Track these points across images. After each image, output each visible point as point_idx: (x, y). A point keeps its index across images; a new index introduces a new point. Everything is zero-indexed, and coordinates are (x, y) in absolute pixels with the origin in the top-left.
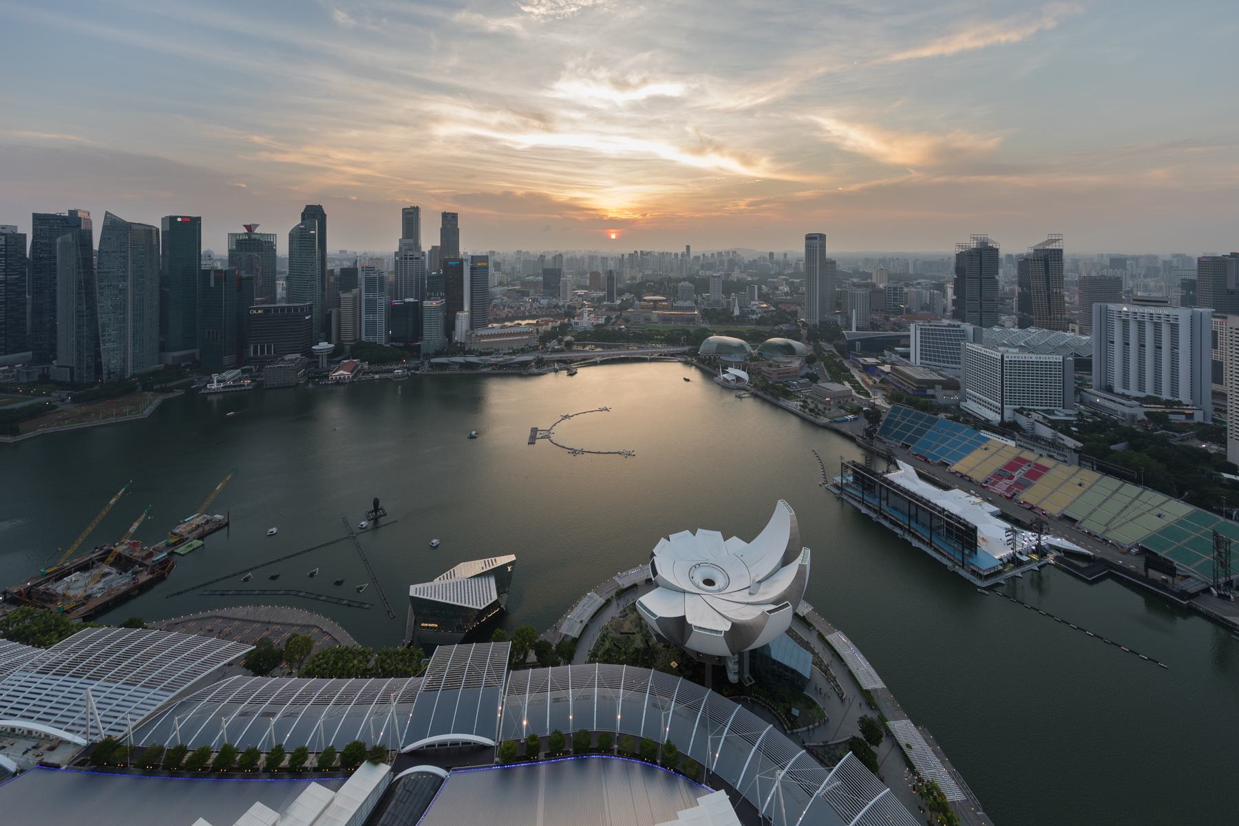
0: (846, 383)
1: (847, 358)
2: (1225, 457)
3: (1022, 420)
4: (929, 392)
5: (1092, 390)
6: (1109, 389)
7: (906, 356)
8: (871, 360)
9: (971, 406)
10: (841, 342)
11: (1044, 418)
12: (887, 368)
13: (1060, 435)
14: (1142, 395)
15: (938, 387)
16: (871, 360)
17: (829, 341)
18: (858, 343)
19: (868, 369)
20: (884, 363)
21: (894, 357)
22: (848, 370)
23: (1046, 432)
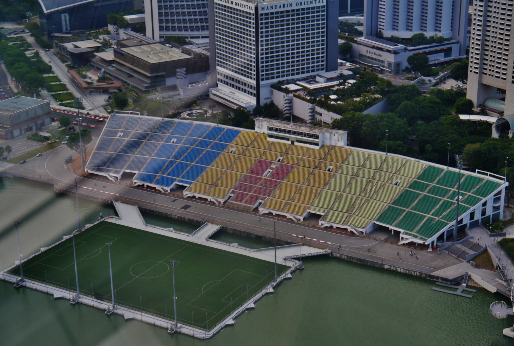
0: (44, 92)
1: (47, 47)
2: (465, 94)
3: (280, 100)
4: (170, 81)
5: (362, 39)
6: (379, 36)
7: (139, 28)
8: (85, 45)
9: (224, 92)
10: (37, 20)
11: (304, 89)
12: (108, 55)
13: (318, 109)
14: (408, 35)
15: (181, 71)
16: (85, 45)
17: (20, 18)
18: (65, 18)
19: (81, 61)
20: (106, 45)
21: (123, 34)
22: (49, 69)
23: (302, 109)
